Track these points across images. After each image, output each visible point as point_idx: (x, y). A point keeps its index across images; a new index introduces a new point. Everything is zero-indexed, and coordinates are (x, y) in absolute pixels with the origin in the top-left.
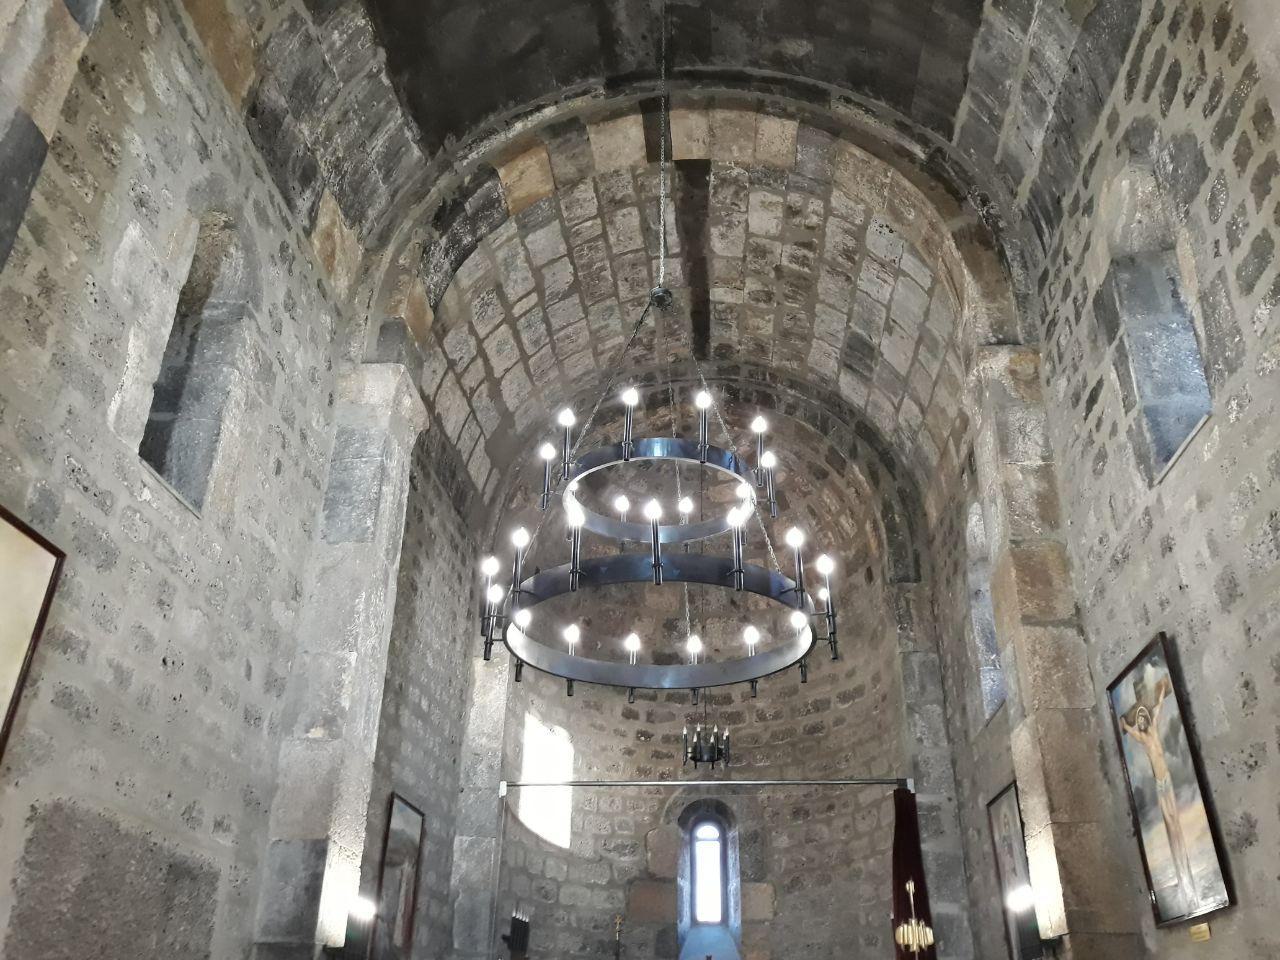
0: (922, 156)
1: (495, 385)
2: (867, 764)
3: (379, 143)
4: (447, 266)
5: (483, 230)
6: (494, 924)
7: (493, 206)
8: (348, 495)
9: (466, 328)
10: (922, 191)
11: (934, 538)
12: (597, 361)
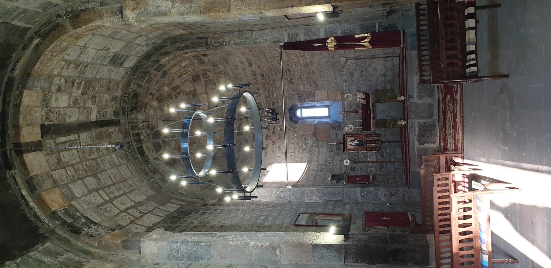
0: (38, 40)
1: (136, 205)
2: (274, 58)
4: (96, 227)
5: (78, 214)
6: (333, 186)
7: (68, 211)
8: (193, 253)
9: (117, 218)
10: (56, 40)
11: (191, 32)
12: (123, 165)
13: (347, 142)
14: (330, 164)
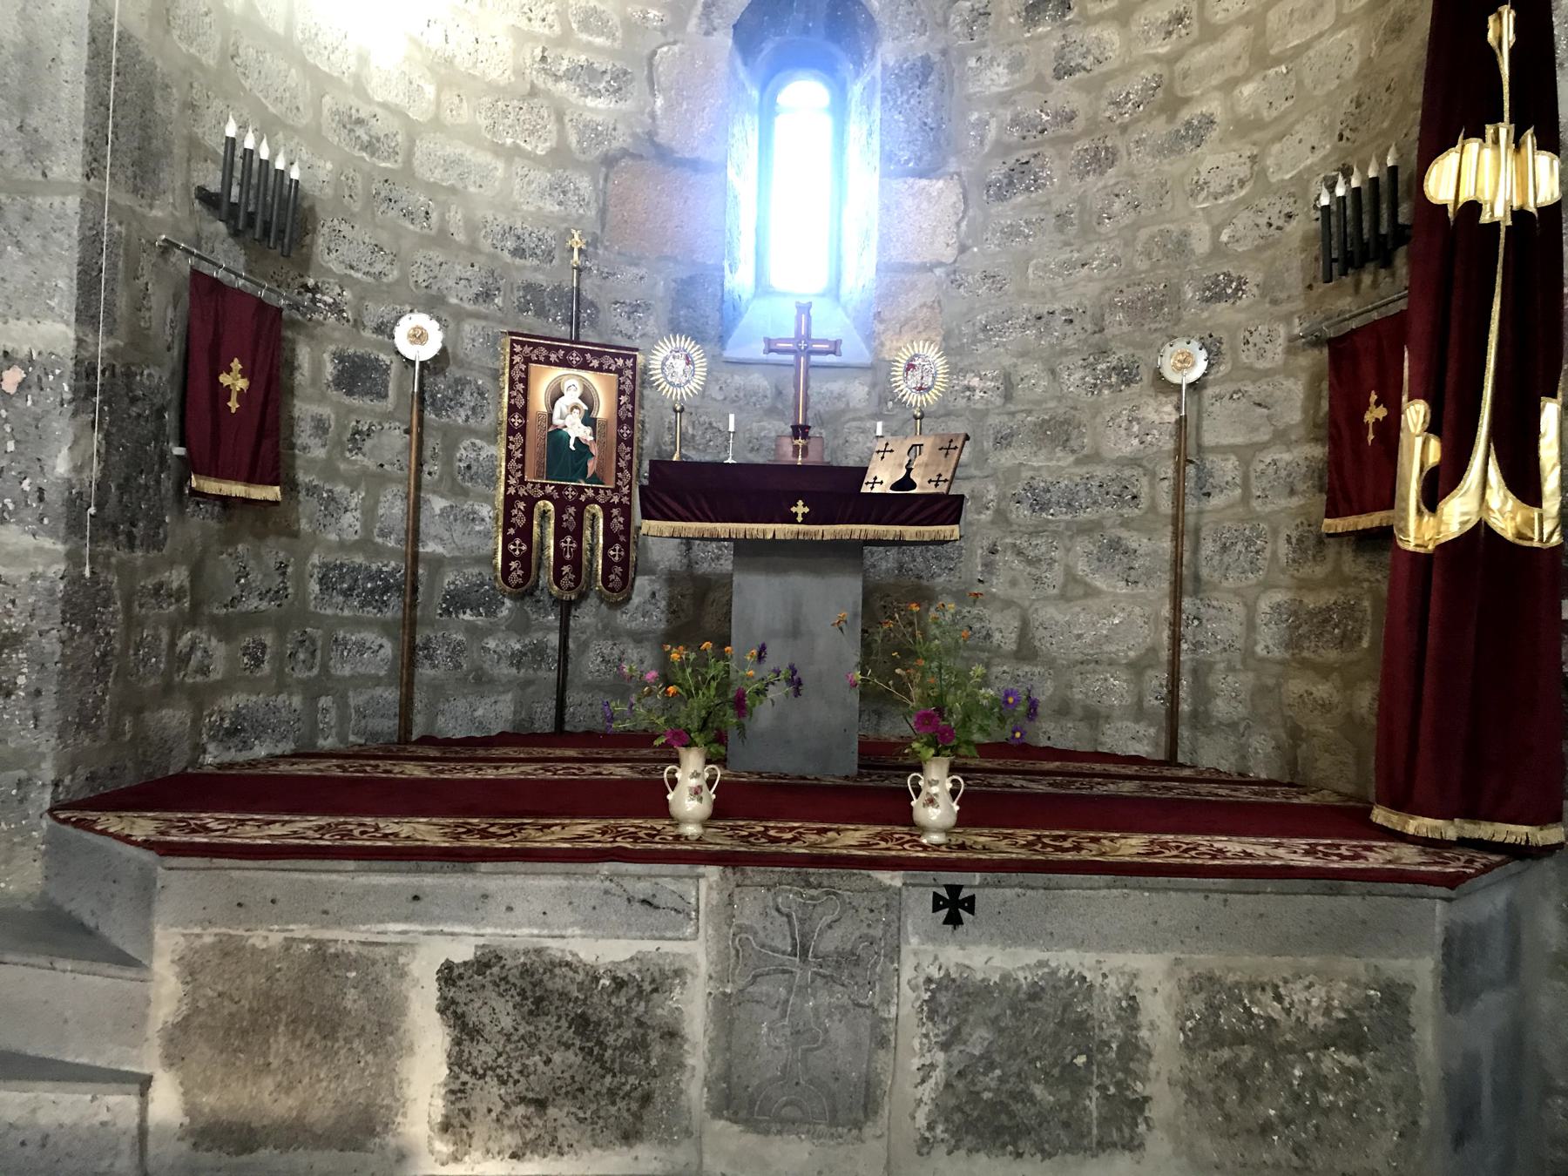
13: (584, 366)
14: (408, 215)
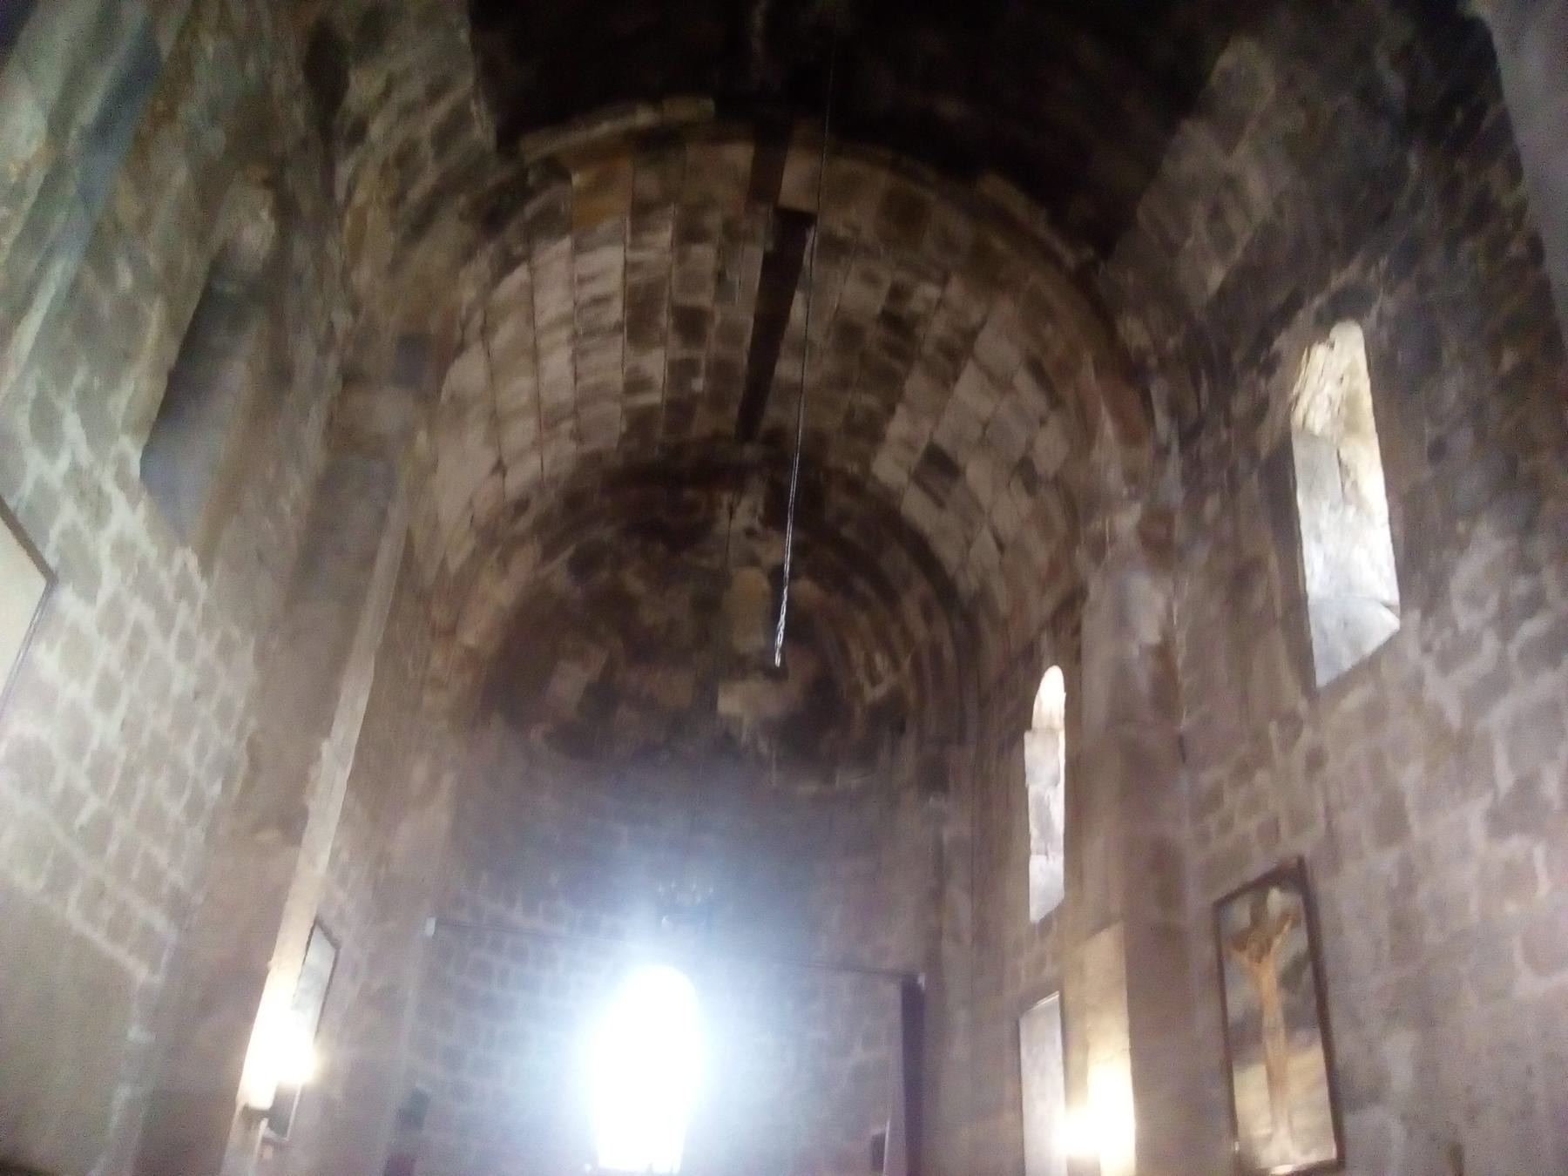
3: (441, 110)
